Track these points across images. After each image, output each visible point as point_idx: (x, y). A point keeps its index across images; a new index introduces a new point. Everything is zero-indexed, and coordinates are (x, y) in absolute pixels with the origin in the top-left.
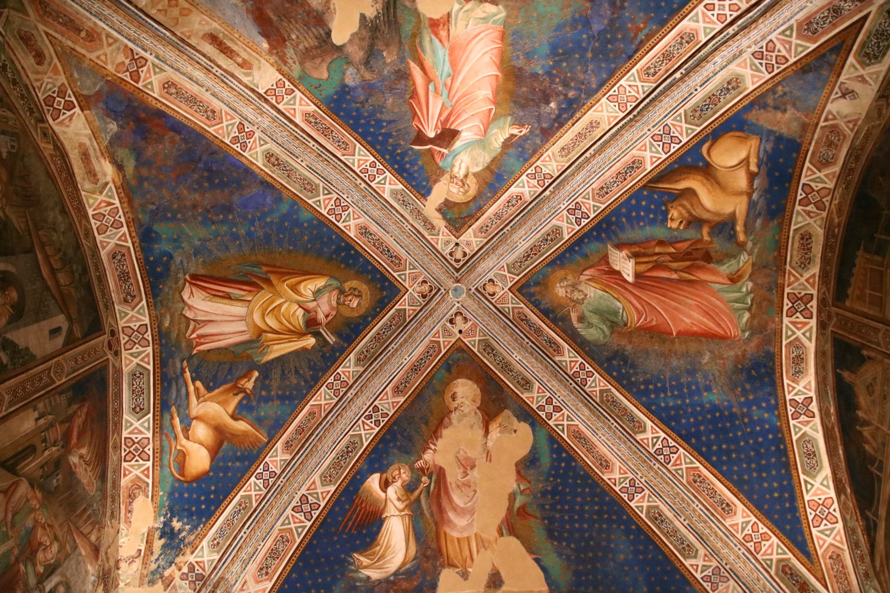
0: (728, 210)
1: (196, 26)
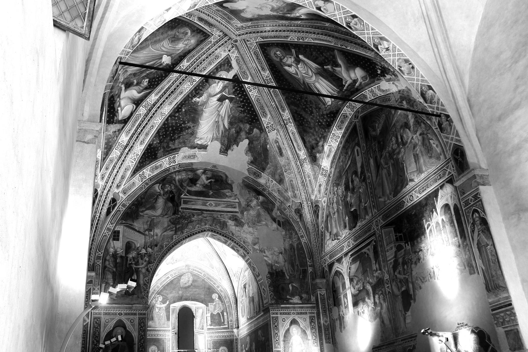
0: (127, 92)
1: (284, 161)
